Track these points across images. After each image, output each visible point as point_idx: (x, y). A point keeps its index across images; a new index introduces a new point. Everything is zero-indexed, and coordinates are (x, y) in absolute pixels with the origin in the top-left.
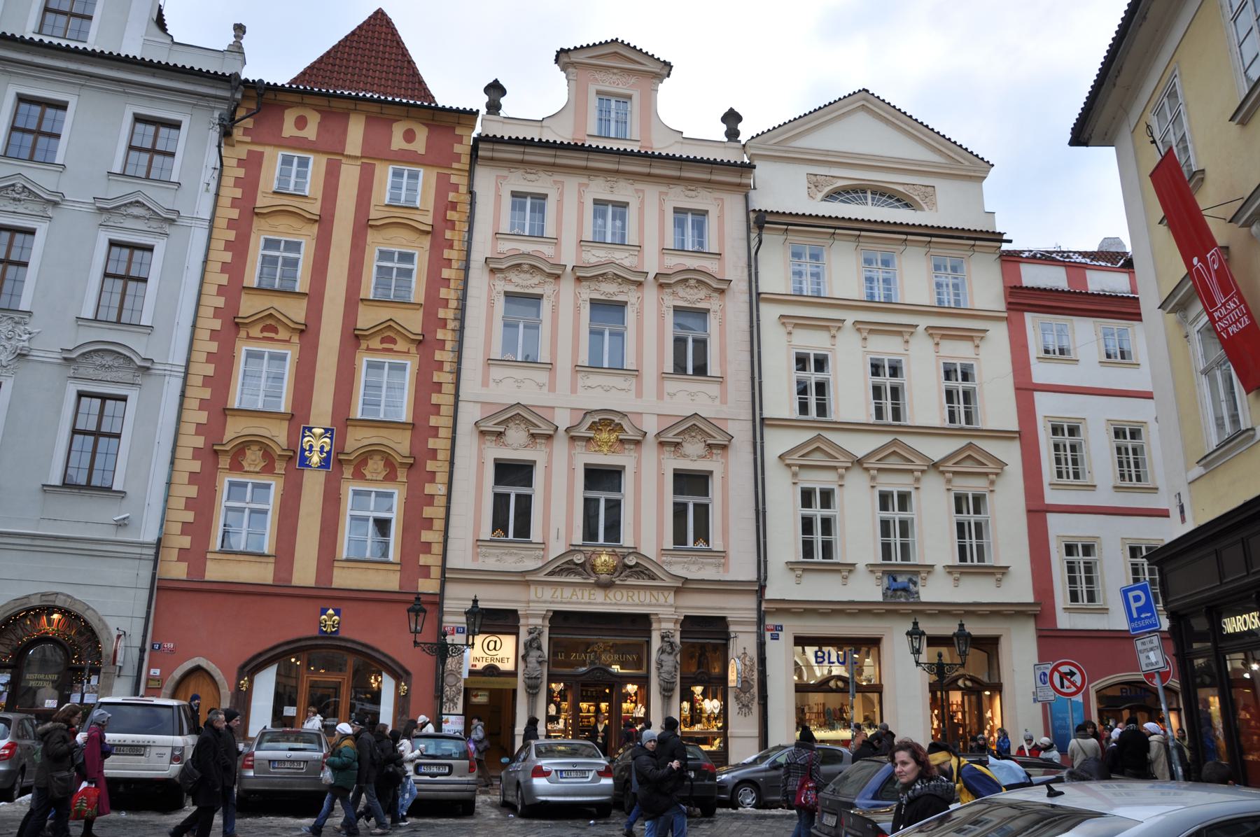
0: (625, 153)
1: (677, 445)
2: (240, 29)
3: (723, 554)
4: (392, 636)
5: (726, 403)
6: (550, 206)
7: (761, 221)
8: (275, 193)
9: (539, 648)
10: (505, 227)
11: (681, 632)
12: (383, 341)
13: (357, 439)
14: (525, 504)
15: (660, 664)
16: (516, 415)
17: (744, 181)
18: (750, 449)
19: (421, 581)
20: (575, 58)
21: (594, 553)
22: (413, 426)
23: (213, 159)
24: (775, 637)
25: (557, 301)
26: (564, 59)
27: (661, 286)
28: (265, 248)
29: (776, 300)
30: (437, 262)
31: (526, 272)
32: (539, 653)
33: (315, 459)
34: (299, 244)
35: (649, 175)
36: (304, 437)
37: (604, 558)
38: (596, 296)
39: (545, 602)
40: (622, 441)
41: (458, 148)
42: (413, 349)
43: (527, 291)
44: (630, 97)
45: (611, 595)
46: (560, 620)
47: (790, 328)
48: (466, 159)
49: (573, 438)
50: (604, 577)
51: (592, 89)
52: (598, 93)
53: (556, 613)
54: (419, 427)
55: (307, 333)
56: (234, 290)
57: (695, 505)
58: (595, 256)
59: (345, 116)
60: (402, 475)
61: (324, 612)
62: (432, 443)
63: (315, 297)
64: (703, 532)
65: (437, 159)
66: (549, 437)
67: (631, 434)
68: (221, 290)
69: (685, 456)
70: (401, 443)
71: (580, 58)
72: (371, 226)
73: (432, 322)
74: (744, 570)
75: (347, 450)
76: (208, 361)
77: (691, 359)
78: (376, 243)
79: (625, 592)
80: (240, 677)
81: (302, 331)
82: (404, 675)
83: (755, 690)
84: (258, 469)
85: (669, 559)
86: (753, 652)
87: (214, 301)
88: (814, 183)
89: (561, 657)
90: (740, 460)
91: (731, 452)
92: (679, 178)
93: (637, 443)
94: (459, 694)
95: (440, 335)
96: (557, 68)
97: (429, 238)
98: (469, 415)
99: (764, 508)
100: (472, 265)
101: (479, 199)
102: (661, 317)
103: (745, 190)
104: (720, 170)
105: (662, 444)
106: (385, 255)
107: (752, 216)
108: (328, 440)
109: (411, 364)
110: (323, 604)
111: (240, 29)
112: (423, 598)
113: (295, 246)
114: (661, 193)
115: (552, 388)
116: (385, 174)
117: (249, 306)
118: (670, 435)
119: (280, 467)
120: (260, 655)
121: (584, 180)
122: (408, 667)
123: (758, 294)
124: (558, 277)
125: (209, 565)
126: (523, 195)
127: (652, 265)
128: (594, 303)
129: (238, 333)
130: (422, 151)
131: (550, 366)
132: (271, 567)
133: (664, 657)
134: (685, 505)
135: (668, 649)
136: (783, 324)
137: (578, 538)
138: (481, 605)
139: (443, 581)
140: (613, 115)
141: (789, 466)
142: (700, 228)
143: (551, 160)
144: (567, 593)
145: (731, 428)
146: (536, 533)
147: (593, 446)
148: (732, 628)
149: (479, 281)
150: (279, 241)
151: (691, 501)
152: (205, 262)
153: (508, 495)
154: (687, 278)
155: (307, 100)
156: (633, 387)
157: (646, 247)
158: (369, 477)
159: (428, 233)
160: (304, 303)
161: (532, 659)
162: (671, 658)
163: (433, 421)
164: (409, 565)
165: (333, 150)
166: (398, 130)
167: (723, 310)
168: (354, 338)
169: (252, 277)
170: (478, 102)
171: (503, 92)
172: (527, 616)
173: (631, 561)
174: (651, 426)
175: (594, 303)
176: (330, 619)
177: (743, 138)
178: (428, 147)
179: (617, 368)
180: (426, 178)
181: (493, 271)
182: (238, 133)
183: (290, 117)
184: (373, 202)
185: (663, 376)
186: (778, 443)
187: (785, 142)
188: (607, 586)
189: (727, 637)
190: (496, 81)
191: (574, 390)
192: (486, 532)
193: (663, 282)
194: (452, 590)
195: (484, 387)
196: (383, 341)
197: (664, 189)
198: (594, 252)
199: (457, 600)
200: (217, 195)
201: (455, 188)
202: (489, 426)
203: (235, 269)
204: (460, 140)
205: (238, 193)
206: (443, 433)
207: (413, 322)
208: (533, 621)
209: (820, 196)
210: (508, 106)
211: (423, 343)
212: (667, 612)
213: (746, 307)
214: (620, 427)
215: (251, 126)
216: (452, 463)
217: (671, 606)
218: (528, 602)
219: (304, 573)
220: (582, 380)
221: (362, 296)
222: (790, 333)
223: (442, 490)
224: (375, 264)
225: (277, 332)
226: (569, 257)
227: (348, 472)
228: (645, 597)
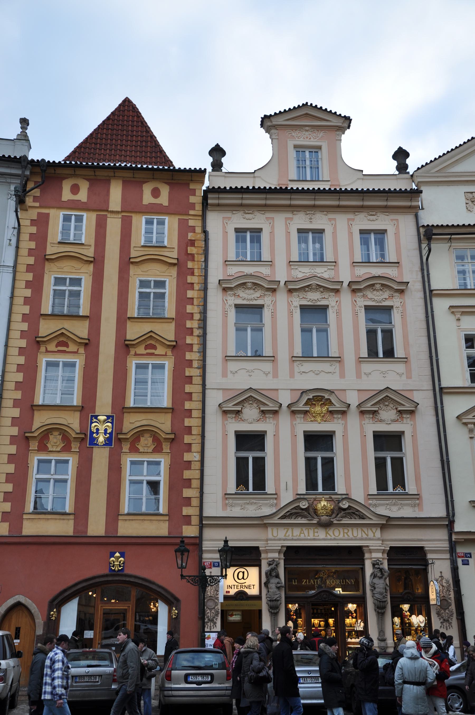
0: (319, 191)
1: (374, 413)
2: (24, 122)
3: (417, 496)
4: (163, 571)
5: (411, 378)
6: (265, 237)
7: (429, 234)
8: (60, 243)
9: (277, 576)
10: (232, 256)
11: (388, 560)
13: (131, 423)
14: (260, 464)
15: (373, 587)
16: (250, 397)
17: (414, 204)
18: (432, 412)
19: (184, 527)
20: (275, 121)
21: (315, 499)
22: (172, 410)
23: (12, 221)
24: (466, 563)
25: (275, 309)
26: (268, 123)
27: (354, 291)
28: (55, 285)
29: (446, 294)
30: (183, 286)
31: (250, 289)
32: (277, 580)
33: (101, 439)
34: (80, 279)
35: (339, 206)
36: (92, 423)
37: (323, 503)
38: (305, 302)
39: (280, 540)
40: (331, 412)
41: (192, 199)
42: (169, 353)
43: (251, 303)
44: (320, 148)
45: (331, 532)
46: (292, 553)
47: (458, 316)
48: (199, 207)
49: (294, 412)
50: (324, 518)
52: (295, 147)
53: (288, 548)
54: (177, 411)
55: (90, 345)
56: (34, 317)
57: (392, 459)
58: (302, 272)
59: (107, 182)
60: (166, 448)
61: (112, 555)
62: (187, 422)
63: (94, 318)
64: (400, 480)
65: (177, 208)
66: (275, 412)
67: (338, 406)
68: (25, 317)
69: (381, 421)
70: (164, 424)
72: (132, 263)
73: (182, 331)
74: (434, 508)
75: (125, 431)
76: (18, 371)
77: (381, 346)
78: (136, 275)
79: (341, 530)
80: (50, 609)
81: (86, 344)
82: (175, 602)
83: (453, 607)
84: (59, 449)
85: (375, 502)
86: (448, 575)
87: (20, 326)
89: (295, 583)
90: (425, 422)
91: (418, 416)
92: (362, 207)
93: (343, 413)
94: (217, 615)
95: (189, 340)
96: (262, 130)
97: (176, 268)
98: (214, 399)
99: (448, 459)
100: (210, 286)
103: (415, 211)
105: (363, 413)
106: (144, 284)
107: (422, 230)
108: (110, 424)
109: (168, 364)
110: (112, 549)
111: (24, 122)
112: (186, 541)
113: (77, 282)
114: (349, 220)
115: (275, 375)
116: (140, 223)
117: (46, 328)
118: (369, 405)
119: (75, 447)
120: (65, 591)
121: (289, 215)
122: (178, 595)
123: (431, 291)
124: (274, 290)
125: (25, 523)
126: (243, 231)
127: (346, 276)
128: (303, 308)
130: (166, 203)
131: (273, 359)
132: (72, 522)
133: (376, 581)
134: (384, 459)
135: (379, 574)
136: (453, 313)
137: (302, 489)
138: (231, 544)
139: (202, 527)
140: (308, 163)
141: (466, 424)
142: (381, 244)
143: (263, 202)
144: (296, 532)
145: (416, 397)
146: (270, 487)
147: (309, 418)
148: (429, 556)
149: (215, 298)
150: (65, 279)
151: (388, 456)
152: (12, 297)
153: (247, 459)
154: (372, 284)
155: (79, 172)
156: (337, 370)
157: (340, 262)
158: (141, 450)
159: (174, 264)
160: (87, 323)
161: (272, 586)
162: (382, 581)
163: (187, 405)
164: (175, 516)
165: (100, 208)
166: (147, 190)
167: (404, 306)
168: (125, 347)
169: (47, 308)
170: (205, 163)
171: (223, 153)
172: (267, 551)
173: (345, 505)
174: (353, 399)
175: (303, 308)
176: (117, 560)
177: (411, 170)
178: (170, 200)
179: (325, 357)
180: (170, 224)
181: (225, 290)
182: (29, 201)
183: (66, 186)
184: (132, 246)
185: (360, 360)
186: (454, 407)
187: (443, 169)
188: (327, 525)
189: (425, 563)
191: (292, 375)
192: (232, 487)
193: (355, 288)
194: (208, 534)
195: (224, 377)
197: (351, 216)
198: (300, 269)
199: (213, 541)
200: (17, 247)
201: (193, 229)
202: (230, 407)
203: (34, 301)
204: (193, 193)
205: (33, 245)
206: (196, 414)
207: (168, 332)
208: (271, 555)
210: (229, 164)
211: (177, 347)
212: (375, 545)
213: (422, 302)
214: (329, 402)
215: (38, 194)
216: (203, 436)
217: (378, 539)
218: (267, 540)
219: (97, 526)
220: (298, 368)
221: (128, 316)
222: (458, 320)
223: (197, 457)
224: (137, 290)
225: (67, 346)
226: (281, 274)
227: (126, 447)
228: (357, 533)
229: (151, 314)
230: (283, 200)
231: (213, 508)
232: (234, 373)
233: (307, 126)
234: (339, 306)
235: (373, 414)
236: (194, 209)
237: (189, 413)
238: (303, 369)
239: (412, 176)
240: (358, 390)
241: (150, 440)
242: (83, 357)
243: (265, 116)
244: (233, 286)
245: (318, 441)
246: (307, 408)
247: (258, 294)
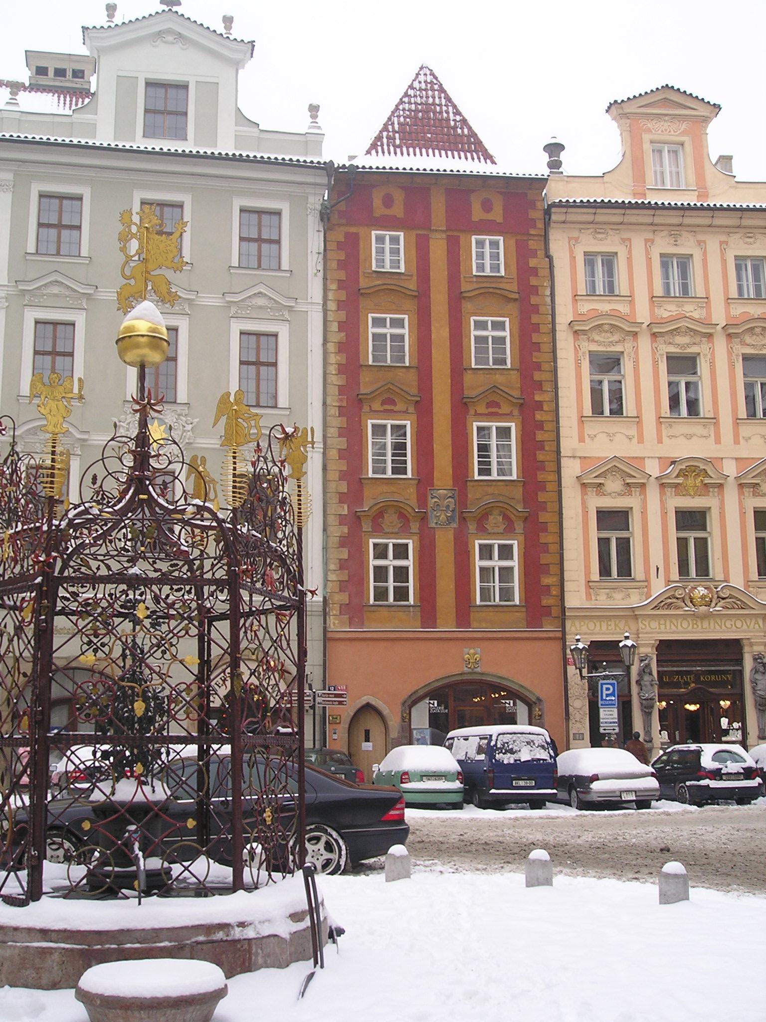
2: (314, 109)
9: (651, 674)
12: (488, 405)
14: (624, 546)
15: (754, 682)
38: (672, 349)
46: (665, 648)
48: (540, 225)
51: (646, 137)
58: (668, 310)
66: (643, 485)
71: (632, 108)
72: (464, 298)
98: (570, 470)
100: (558, 327)
101: (556, 263)
102: (732, 366)
111: (314, 109)
114: (721, 243)
115: (641, 440)
124: (635, 334)
127: (719, 317)
129: (361, 409)
130: (500, 219)
174: (730, 469)
191: (660, 441)
192: (595, 575)
196: (488, 405)
210: (570, 164)
227: (472, 527)
229: (491, 363)
230: (644, 217)
231: (574, 598)
233: (666, 114)
234: (713, 354)
235: (754, 487)
236: (534, 227)
238: (672, 432)
240: (736, 459)
242: (415, 417)
243: (616, 102)
244: (587, 328)
246: (680, 480)
247: (616, 337)
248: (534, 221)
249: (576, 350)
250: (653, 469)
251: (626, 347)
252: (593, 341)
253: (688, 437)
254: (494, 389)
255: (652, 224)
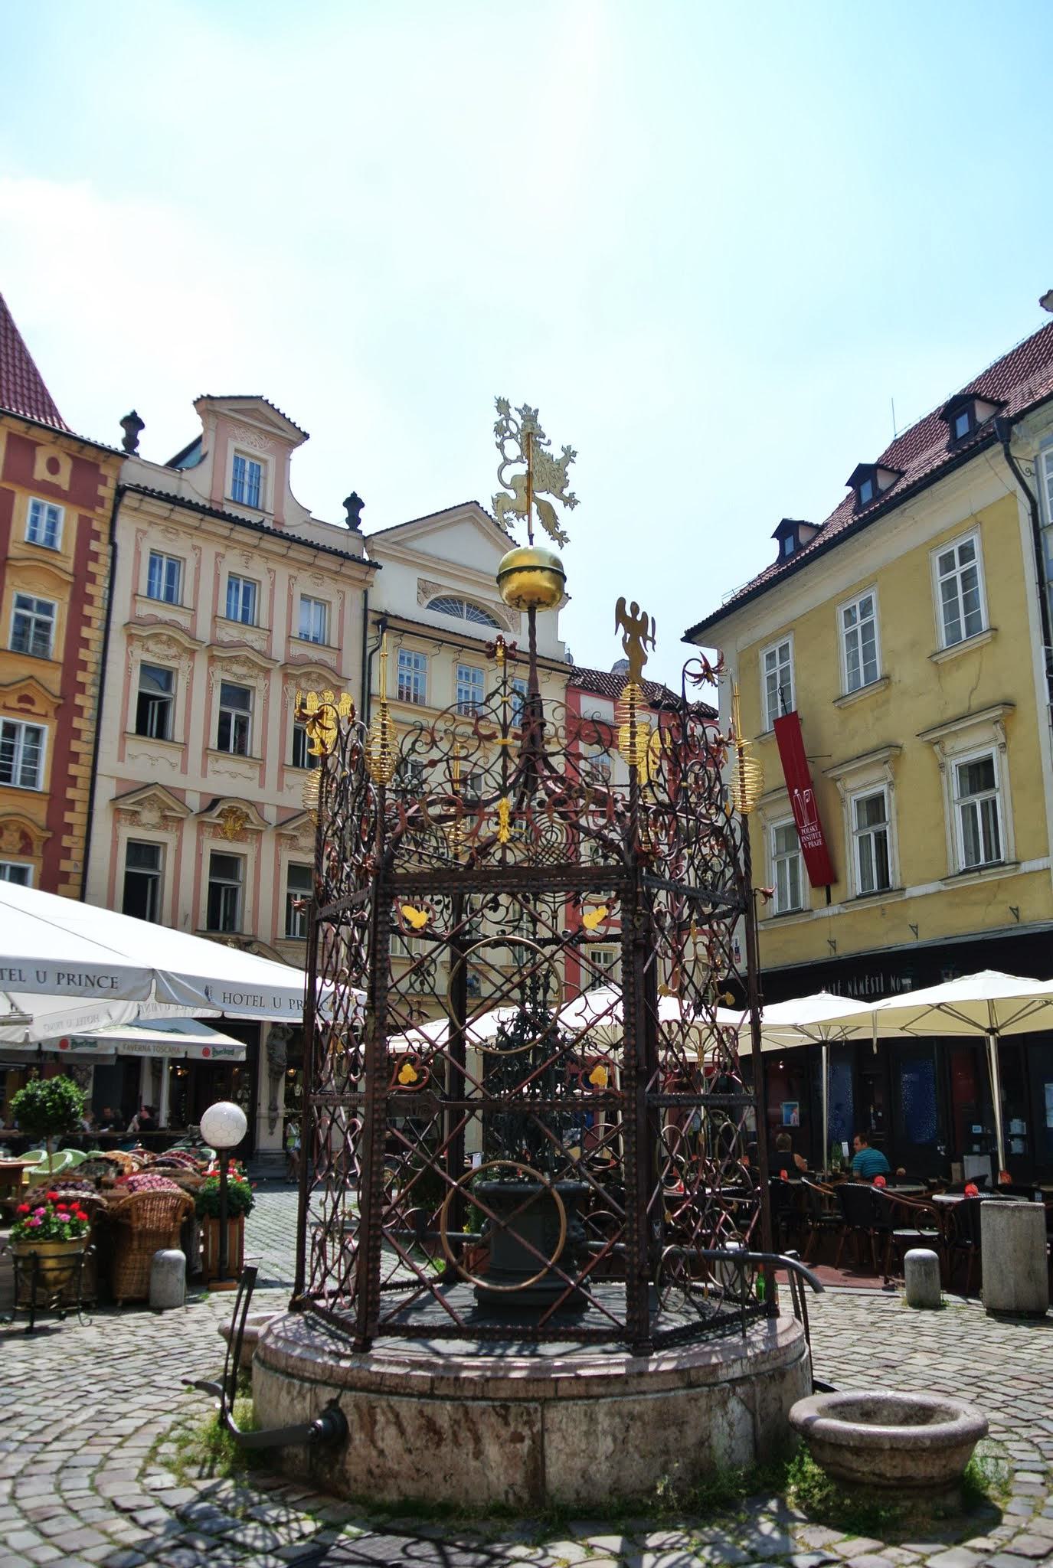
15: (271, 1048)
38: (228, 677)
41: (102, 491)
42: (51, 714)
48: (109, 505)
58: (230, 633)
62: (69, 817)
65: (81, 495)
69: (301, 849)
88: (424, 588)
98: (105, 791)
100: (113, 627)
101: (120, 553)
104: (344, 555)
106: (23, 603)
114: (291, 577)
115: (184, 770)
123: (370, 695)
130: (66, 487)
156: (257, 775)
159: (68, 582)
174: (271, 815)
180: (67, 518)
184: (13, 536)
185: (282, 767)
190: (134, 414)
191: (204, 773)
207: (53, 679)
209: (427, 602)
232: (134, 757)
234: (268, 691)
236: (102, 505)
237: (71, 805)
239: (365, 538)
241: (17, 835)
245: (224, 865)
247: (173, 651)
248: (103, 498)
249: (128, 656)
250: (194, 802)
251: (181, 665)
252: (148, 650)
253: (234, 775)
254: (30, 681)
255: (226, 538)
